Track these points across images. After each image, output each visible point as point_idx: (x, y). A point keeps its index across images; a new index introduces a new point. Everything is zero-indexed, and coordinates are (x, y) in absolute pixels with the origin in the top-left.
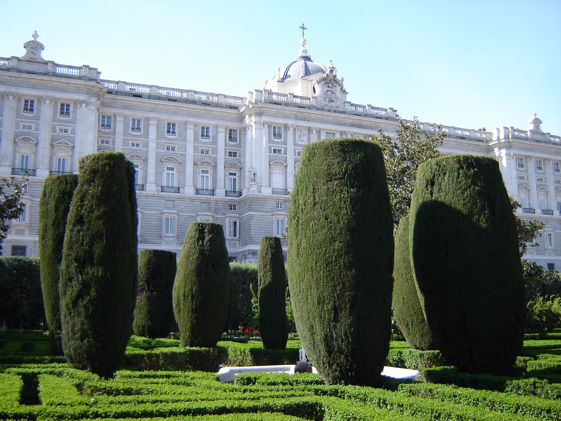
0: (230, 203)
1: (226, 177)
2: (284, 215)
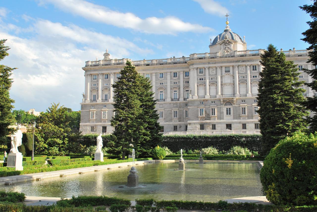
0: (186, 103)
2: (203, 107)
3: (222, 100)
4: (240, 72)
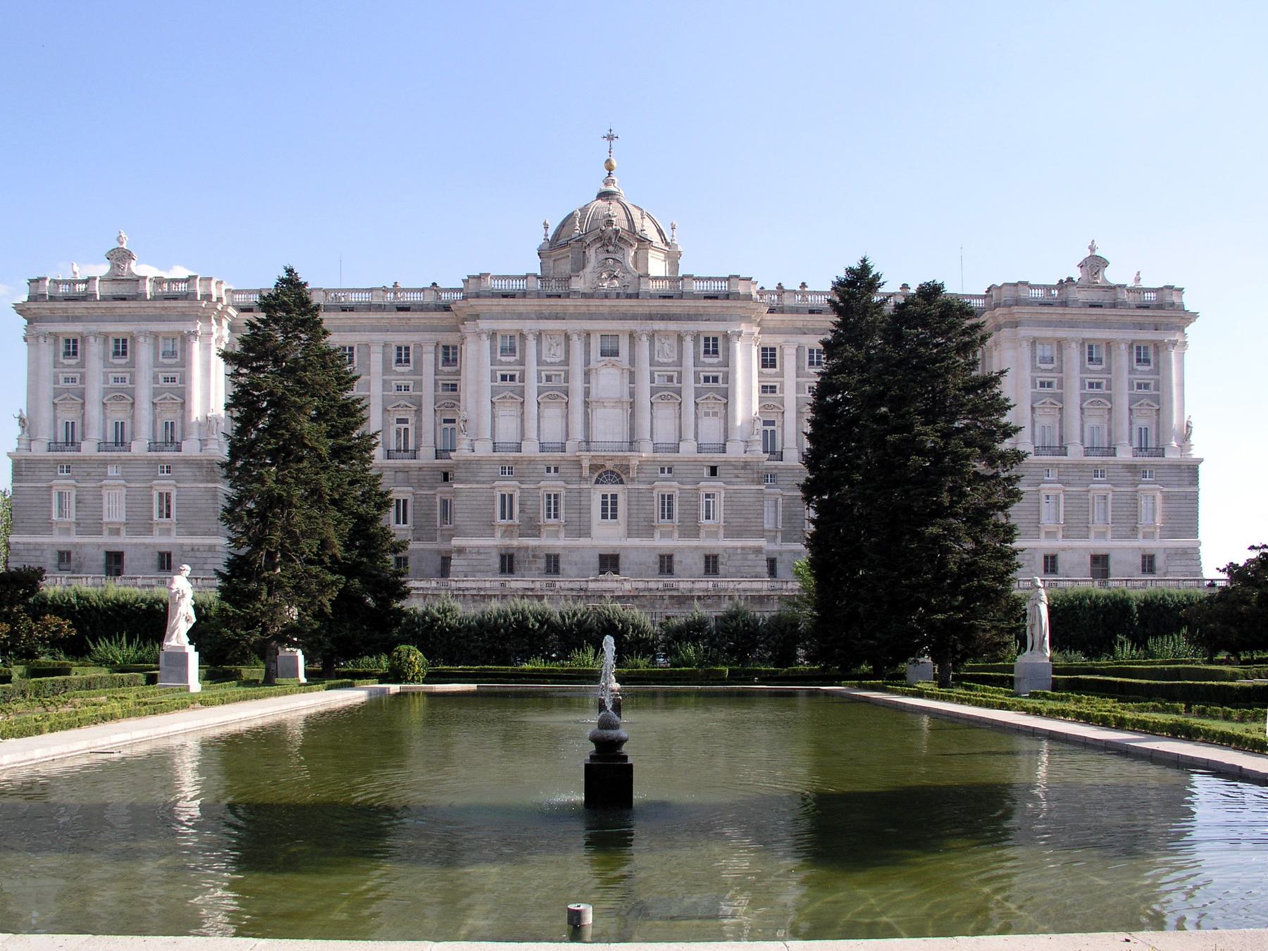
0: (444, 470)
1: (438, 428)
3: (586, 464)
4: (656, 358)
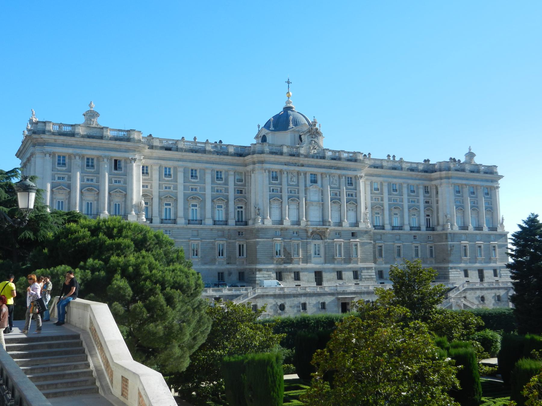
0: (239, 230)
4: (331, 185)
